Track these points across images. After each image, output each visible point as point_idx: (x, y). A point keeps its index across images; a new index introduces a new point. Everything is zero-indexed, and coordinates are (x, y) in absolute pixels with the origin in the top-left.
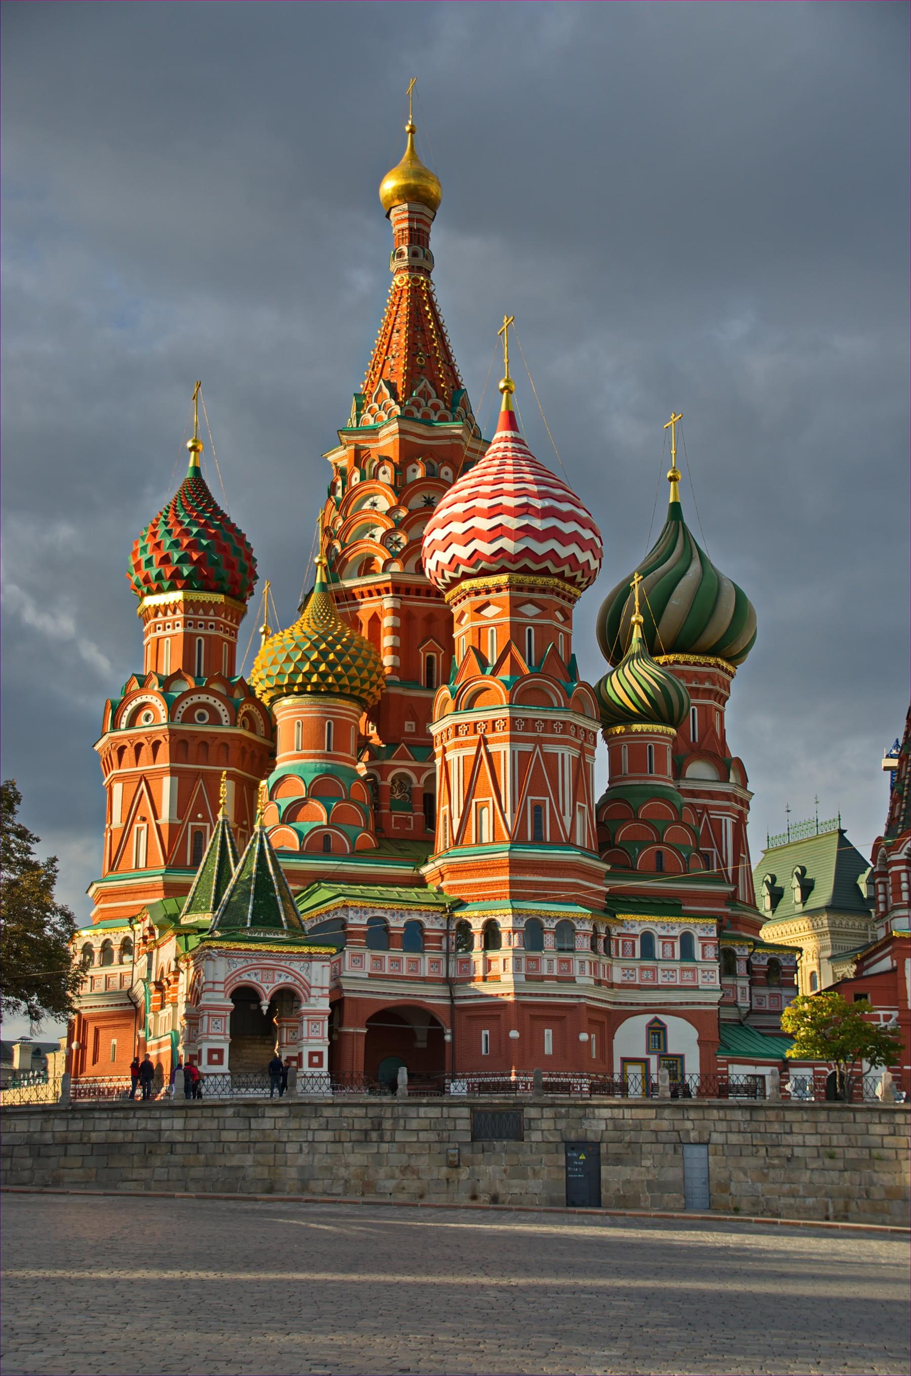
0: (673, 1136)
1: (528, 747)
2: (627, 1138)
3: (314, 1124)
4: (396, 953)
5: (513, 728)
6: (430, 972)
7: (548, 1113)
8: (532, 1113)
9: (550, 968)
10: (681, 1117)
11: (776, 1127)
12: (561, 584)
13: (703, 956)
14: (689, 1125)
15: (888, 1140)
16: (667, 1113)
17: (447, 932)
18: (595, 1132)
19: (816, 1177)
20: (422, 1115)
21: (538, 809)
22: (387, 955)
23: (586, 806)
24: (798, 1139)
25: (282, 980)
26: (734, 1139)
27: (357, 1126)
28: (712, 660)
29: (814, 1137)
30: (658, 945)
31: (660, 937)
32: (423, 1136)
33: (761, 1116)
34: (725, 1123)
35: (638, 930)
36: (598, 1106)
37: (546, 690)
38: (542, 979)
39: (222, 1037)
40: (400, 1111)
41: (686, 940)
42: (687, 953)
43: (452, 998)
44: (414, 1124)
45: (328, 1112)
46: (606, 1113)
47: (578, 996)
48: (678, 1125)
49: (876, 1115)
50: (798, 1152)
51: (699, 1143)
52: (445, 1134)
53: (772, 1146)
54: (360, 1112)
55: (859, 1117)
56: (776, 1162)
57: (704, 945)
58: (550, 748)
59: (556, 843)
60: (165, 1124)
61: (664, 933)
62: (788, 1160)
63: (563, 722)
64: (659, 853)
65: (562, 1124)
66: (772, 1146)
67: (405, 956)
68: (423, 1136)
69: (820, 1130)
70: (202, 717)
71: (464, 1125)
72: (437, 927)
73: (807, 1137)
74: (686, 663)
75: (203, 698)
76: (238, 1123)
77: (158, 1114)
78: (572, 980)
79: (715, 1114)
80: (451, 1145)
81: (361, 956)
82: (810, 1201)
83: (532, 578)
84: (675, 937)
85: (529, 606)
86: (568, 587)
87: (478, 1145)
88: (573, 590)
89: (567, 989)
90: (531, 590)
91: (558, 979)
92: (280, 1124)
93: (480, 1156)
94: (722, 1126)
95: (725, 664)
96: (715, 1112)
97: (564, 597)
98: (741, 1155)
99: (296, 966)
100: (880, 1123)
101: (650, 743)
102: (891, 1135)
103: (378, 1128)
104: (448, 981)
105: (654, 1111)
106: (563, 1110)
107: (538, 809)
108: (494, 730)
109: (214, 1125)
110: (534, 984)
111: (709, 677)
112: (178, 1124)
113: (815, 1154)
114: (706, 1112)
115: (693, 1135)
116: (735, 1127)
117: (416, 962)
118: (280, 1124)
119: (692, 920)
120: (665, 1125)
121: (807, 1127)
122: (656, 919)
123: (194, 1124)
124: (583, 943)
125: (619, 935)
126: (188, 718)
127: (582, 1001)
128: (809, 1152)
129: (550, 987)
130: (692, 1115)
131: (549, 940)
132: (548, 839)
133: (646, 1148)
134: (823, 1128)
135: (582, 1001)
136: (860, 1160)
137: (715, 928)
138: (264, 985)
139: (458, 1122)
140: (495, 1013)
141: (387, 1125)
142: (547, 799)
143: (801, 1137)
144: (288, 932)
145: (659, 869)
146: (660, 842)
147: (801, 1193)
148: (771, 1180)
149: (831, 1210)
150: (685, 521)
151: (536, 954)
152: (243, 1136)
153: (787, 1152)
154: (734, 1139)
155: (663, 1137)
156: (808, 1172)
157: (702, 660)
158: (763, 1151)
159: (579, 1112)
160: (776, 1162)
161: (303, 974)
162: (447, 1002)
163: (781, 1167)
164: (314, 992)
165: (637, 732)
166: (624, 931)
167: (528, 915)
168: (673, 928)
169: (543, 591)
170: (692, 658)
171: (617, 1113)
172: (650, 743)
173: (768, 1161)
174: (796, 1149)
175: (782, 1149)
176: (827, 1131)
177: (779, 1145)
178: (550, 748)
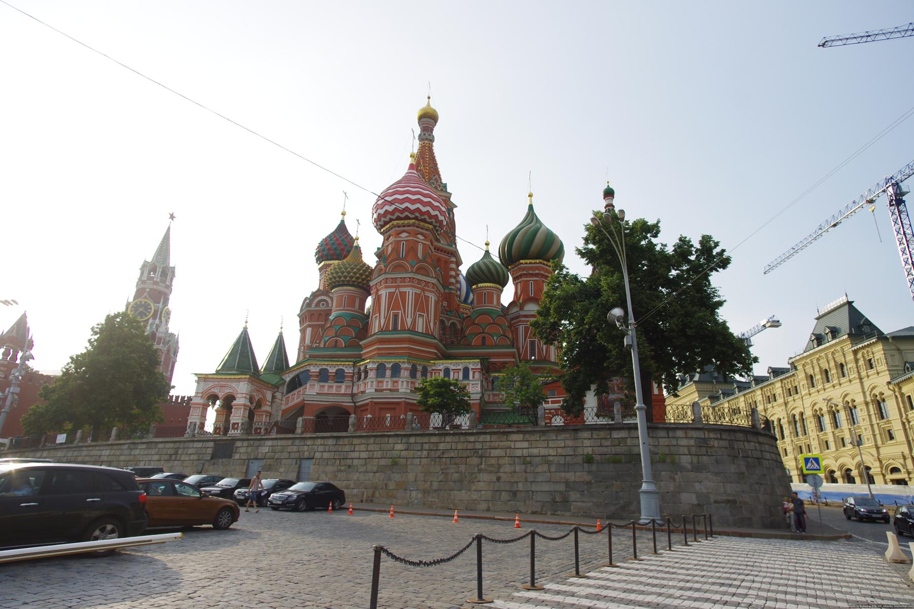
0: (297, 455)
1: (393, 290)
2: (276, 457)
3: (153, 452)
4: (331, 383)
5: (386, 282)
6: (345, 391)
7: (245, 443)
8: (238, 444)
9: (387, 385)
10: (302, 444)
11: (347, 448)
12: (417, 222)
13: (473, 377)
14: (306, 448)
15: (403, 453)
16: (297, 442)
17: (353, 373)
18: (262, 453)
19: (362, 477)
20: (194, 446)
21: (396, 316)
22: (326, 385)
23: (425, 315)
24: (356, 455)
25: (227, 391)
26: (326, 455)
27: (169, 453)
28: (538, 261)
29: (365, 453)
30: (452, 374)
31: (453, 370)
32: (192, 457)
33: (341, 442)
34: (323, 446)
35: (441, 367)
36: (267, 439)
37: (429, 271)
38: (382, 390)
39: (196, 417)
40: (186, 445)
41: (466, 371)
42: (466, 376)
43: (355, 403)
44: (190, 451)
45: (160, 446)
46: (269, 443)
47: (402, 398)
48: (301, 448)
49: (400, 438)
50: (356, 462)
51: (308, 459)
52: (201, 456)
53: (343, 459)
54: (171, 445)
55: (391, 440)
56: (343, 468)
57: (474, 373)
58: (402, 290)
59: (403, 330)
60: (103, 453)
61: (454, 368)
62: (349, 466)
63: (409, 278)
64: (484, 337)
65: (250, 449)
66: (343, 459)
67: (335, 385)
68: (192, 457)
69: (369, 449)
70: (323, 305)
71: (210, 451)
72: (351, 372)
73: (362, 453)
74: (526, 263)
75: (323, 297)
76: (127, 452)
77: (102, 448)
78: (397, 390)
79: (319, 441)
80: (202, 462)
81: (314, 385)
82: (355, 491)
83: (403, 221)
84: (460, 369)
85: (404, 233)
86: (422, 223)
87: (213, 461)
88: (426, 225)
89: (395, 395)
90: (404, 226)
91: (390, 390)
92: (142, 452)
93: (211, 467)
94: (321, 448)
95: (545, 262)
96: (320, 440)
97: (422, 228)
98: (327, 465)
99: (234, 385)
100: (401, 443)
101: (485, 291)
102: (405, 450)
103: (176, 454)
104: (353, 395)
105: (291, 441)
106: (252, 442)
107: (396, 316)
108: (381, 284)
109: (118, 453)
110: (380, 393)
111: (537, 268)
112: (108, 452)
113: (364, 463)
114: (316, 440)
115: (306, 454)
116: (327, 448)
117: (340, 387)
118: (142, 452)
119: (467, 361)
120: (295, 449)
121: (363, 447)
122: (450, 361)
123: (113, 451)
124: (405, 374)
125: (432, 370)
126: (318, 304)
127: (403, 400)
128: (362, 462)
129: (387, 394)
130: (309, 442)
131: (388, 373)
132: (399, 329)
133: (284, 461)
134: (371, 447)
135: (403, 400)
136: (386, 466)
137: (479, 364)
138: (220, 394)
139: (208, 449)
140: (366, 408)
141: (180, 451)
142: (400, 312)
143: (358, 453)
144: (237, 371)
145: (483, 344)
146: (483, 333)
147: (352, 486)
148: (338, 479)
149: (365, 496)
150: (535, 211)
151: (382, 379)
152: (128, 458)
153: (349, 462)
154: (326, 455)
155: (293, 455)
156: (358, 474)
157: (533, 261)
158: (338, 462)
159: (257, 443)
160: (343, 468)
161: (236, 388)
162: (353, 404)
163: (345, 471)
164: (239, 396)
165: (481, 287)
166: (435, 368)
167: (378, 362)
168: (459, 365)
169: (409, 226)
170: (528, 261)
171: (275, 443)
172: (485, 291)
173: (339, 467)
174: (354, 460)
175: (348, 461)
176: (373, 449)
177: (346, 459)
178: (402, 290)
